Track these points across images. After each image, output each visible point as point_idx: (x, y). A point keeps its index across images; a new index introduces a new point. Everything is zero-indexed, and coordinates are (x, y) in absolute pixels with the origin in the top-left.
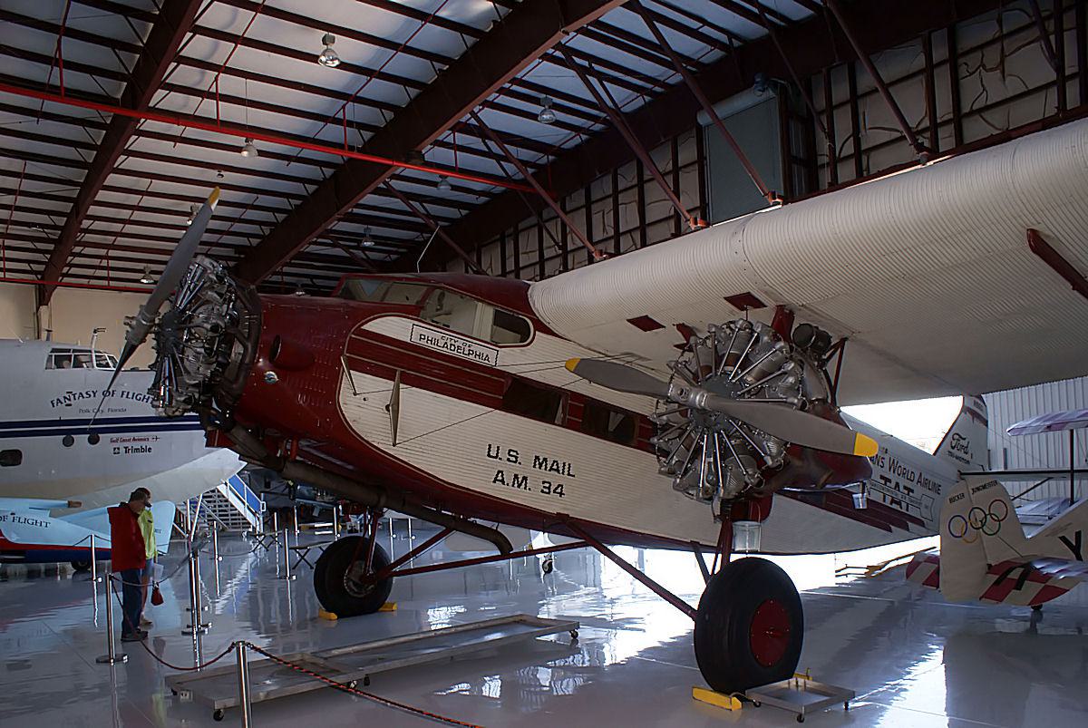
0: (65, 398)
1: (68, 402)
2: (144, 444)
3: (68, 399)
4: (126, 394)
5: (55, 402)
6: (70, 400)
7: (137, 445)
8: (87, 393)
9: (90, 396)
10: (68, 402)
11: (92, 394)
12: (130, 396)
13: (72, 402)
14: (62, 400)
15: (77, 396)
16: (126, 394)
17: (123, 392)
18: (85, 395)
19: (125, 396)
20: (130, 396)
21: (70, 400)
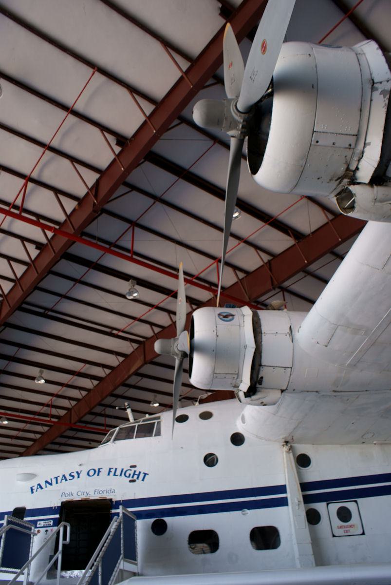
4: (113, 471)
8: (70, 475)
9: (73, 477)
11: (76, 475)
12: (118, 473)
16: (113, 471)
17: (110, 469)
18: (68, 477)
19: (112, 474)
20: (118, 473)
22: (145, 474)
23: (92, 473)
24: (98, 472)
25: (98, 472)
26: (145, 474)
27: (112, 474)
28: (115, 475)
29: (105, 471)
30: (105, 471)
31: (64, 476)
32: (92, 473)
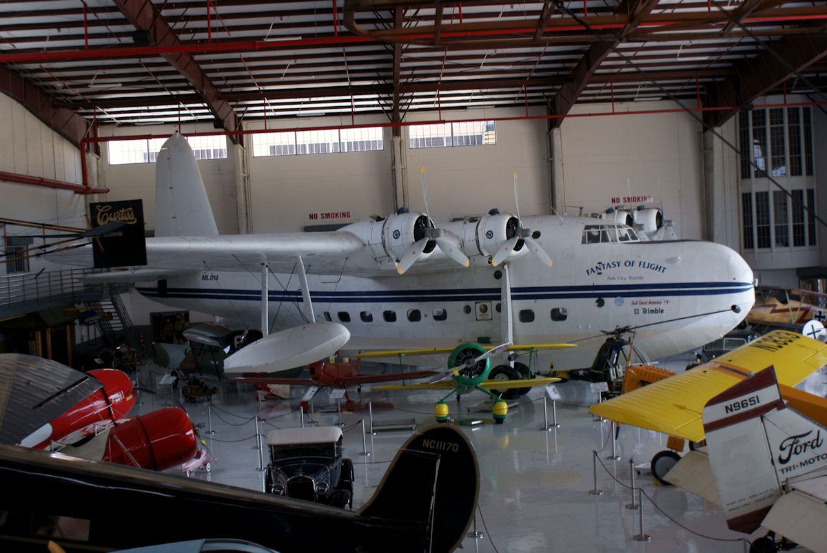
0: (597, 267)
1: (599, 271)
2: (657, 306)
3: (599, 268)
4: (642, 264)
5: (590, 271)
6: (600, 269)
7: (652, 307)
9: (615, 265)
10: (599, 271)
11: (617, 265)
12: (646, 265)
13: (602, 271)
14: (595, 269)
15: (605, 266)
16: (642, 264)
18: (611, 265)
19: (642, 266)
20: (646, 265)
21: (600, 269)
22: (664, 268)
23: (628, 264)
24: (632, 264)
25: (632, 264)
26: (664, 268)
27: (642, 266)
28: (644, 266)
29: (637, 264)
30: (637, 264)
31: (608, 264)
32: (628, 264)
